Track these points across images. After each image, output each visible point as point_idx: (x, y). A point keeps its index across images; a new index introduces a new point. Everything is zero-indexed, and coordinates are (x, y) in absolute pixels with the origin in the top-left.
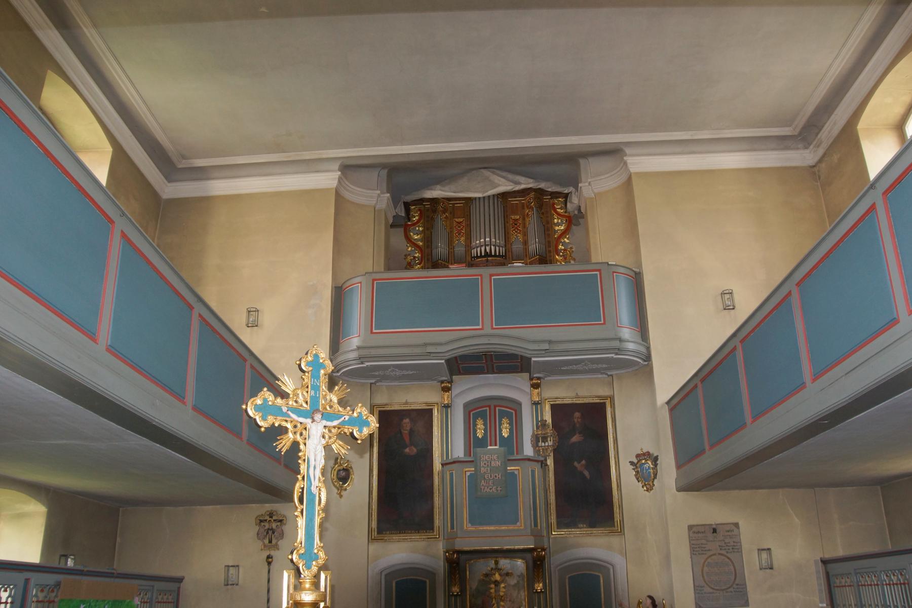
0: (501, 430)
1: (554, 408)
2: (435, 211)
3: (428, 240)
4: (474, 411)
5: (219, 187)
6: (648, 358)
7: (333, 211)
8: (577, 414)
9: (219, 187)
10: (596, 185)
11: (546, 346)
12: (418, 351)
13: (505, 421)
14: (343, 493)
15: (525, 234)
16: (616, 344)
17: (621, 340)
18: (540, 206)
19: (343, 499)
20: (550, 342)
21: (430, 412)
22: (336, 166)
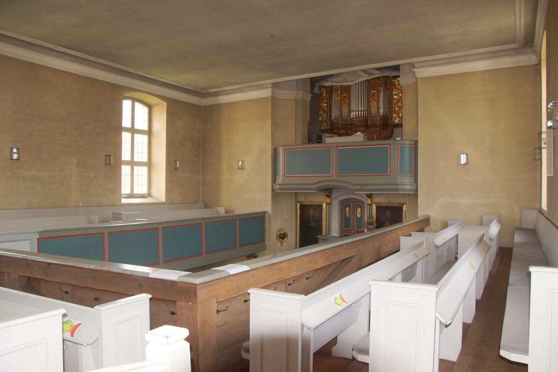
0: (357, 214)
1: (378, 208)
2: (332, 91)
3: (330, 107)
4: (344, 204)
5: (224, 99)
6: (417, 191)
7: (270, 109)
8: (388, 212)
9: (224, 99)
10: (404, 80)
11: (359, 187)
12: (303, 187)
13: (359, 209)
14: (284, 244)
15: (378, 102)
16: (394, 187)
17: (397, 185)
18: (386, 85)
19: (283, 247)
20: (362, 185)
21: (321, 206)
22: (270, 86)
